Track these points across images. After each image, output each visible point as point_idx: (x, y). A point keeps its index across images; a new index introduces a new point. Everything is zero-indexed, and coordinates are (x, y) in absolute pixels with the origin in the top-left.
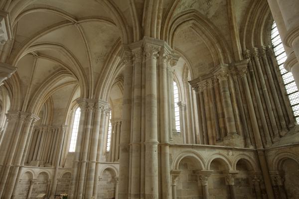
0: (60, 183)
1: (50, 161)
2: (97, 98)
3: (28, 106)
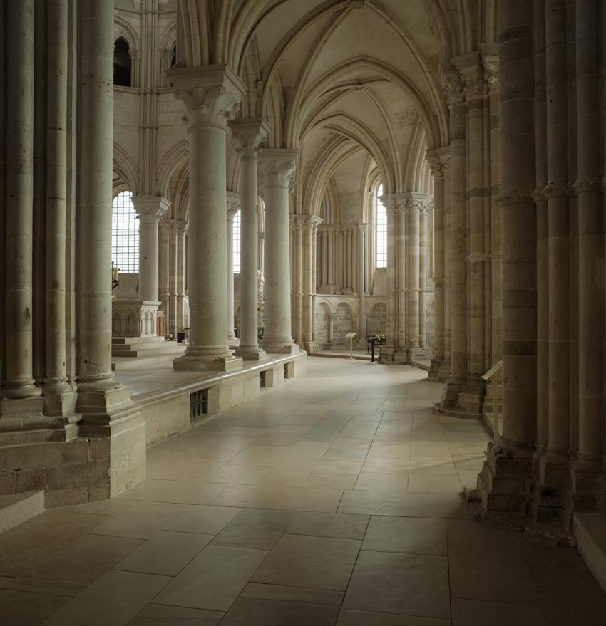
0: (370, 320)
1: (349, 286)
2: (409, 191)
3: (302, 203)
